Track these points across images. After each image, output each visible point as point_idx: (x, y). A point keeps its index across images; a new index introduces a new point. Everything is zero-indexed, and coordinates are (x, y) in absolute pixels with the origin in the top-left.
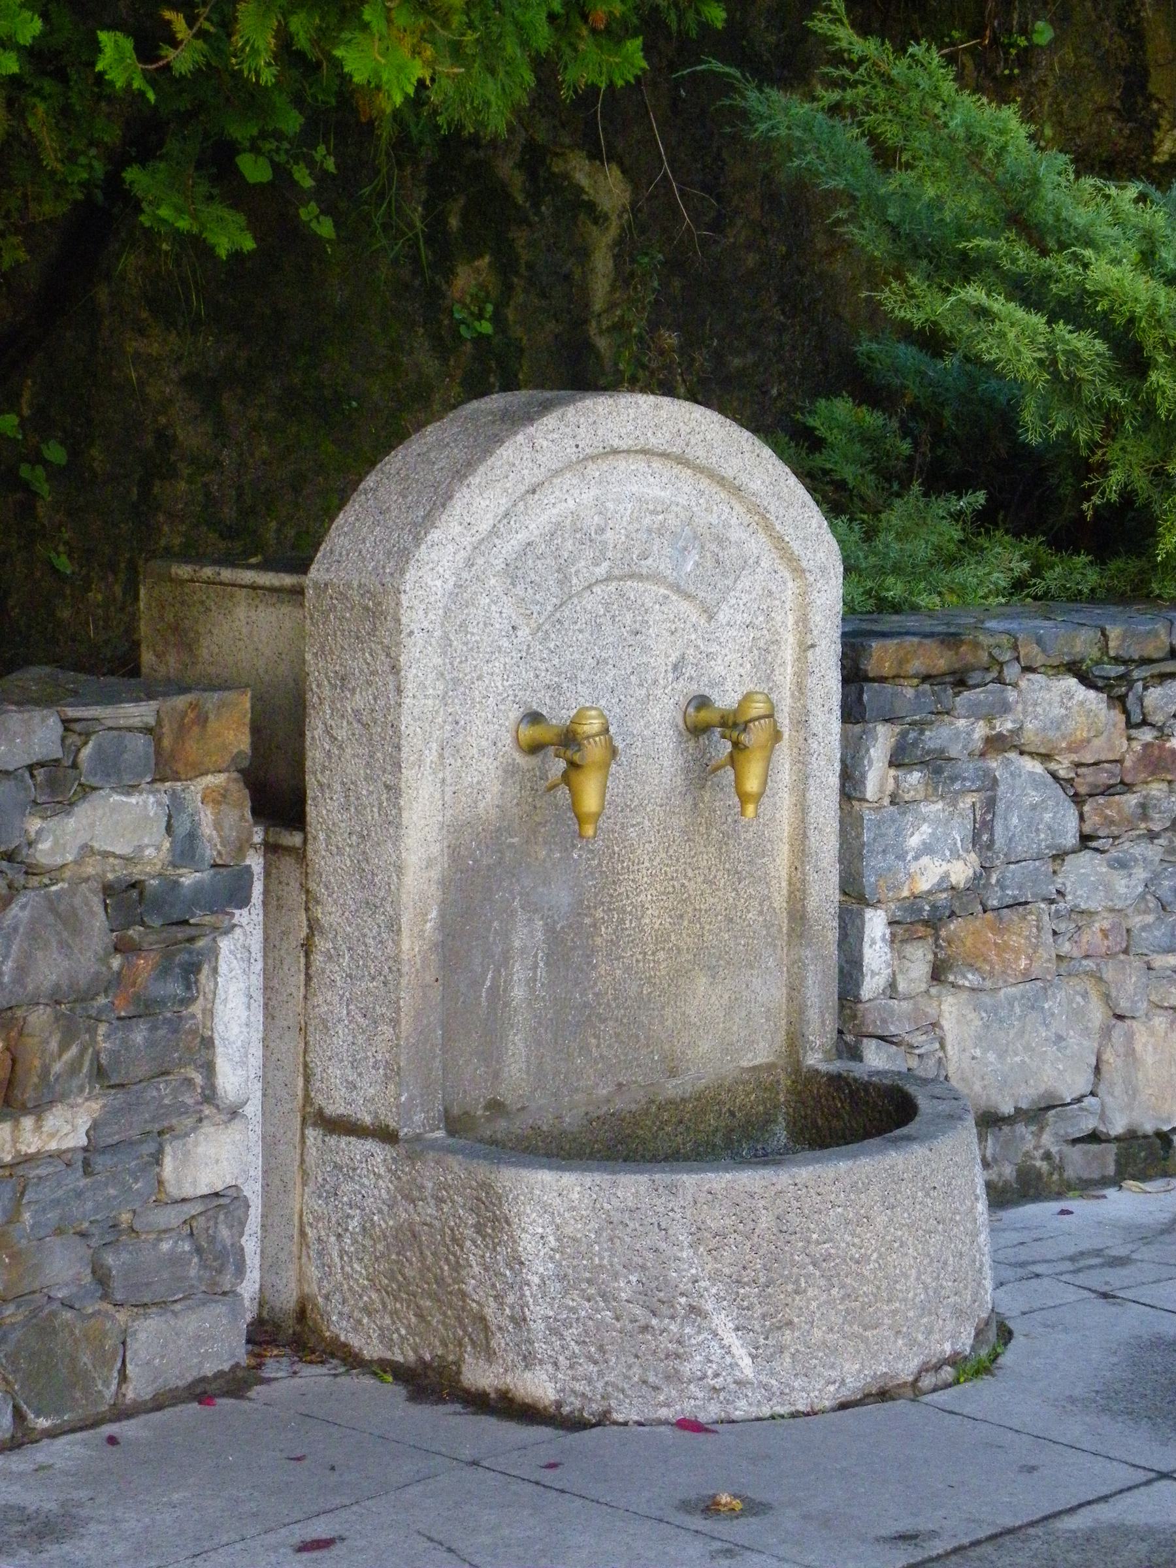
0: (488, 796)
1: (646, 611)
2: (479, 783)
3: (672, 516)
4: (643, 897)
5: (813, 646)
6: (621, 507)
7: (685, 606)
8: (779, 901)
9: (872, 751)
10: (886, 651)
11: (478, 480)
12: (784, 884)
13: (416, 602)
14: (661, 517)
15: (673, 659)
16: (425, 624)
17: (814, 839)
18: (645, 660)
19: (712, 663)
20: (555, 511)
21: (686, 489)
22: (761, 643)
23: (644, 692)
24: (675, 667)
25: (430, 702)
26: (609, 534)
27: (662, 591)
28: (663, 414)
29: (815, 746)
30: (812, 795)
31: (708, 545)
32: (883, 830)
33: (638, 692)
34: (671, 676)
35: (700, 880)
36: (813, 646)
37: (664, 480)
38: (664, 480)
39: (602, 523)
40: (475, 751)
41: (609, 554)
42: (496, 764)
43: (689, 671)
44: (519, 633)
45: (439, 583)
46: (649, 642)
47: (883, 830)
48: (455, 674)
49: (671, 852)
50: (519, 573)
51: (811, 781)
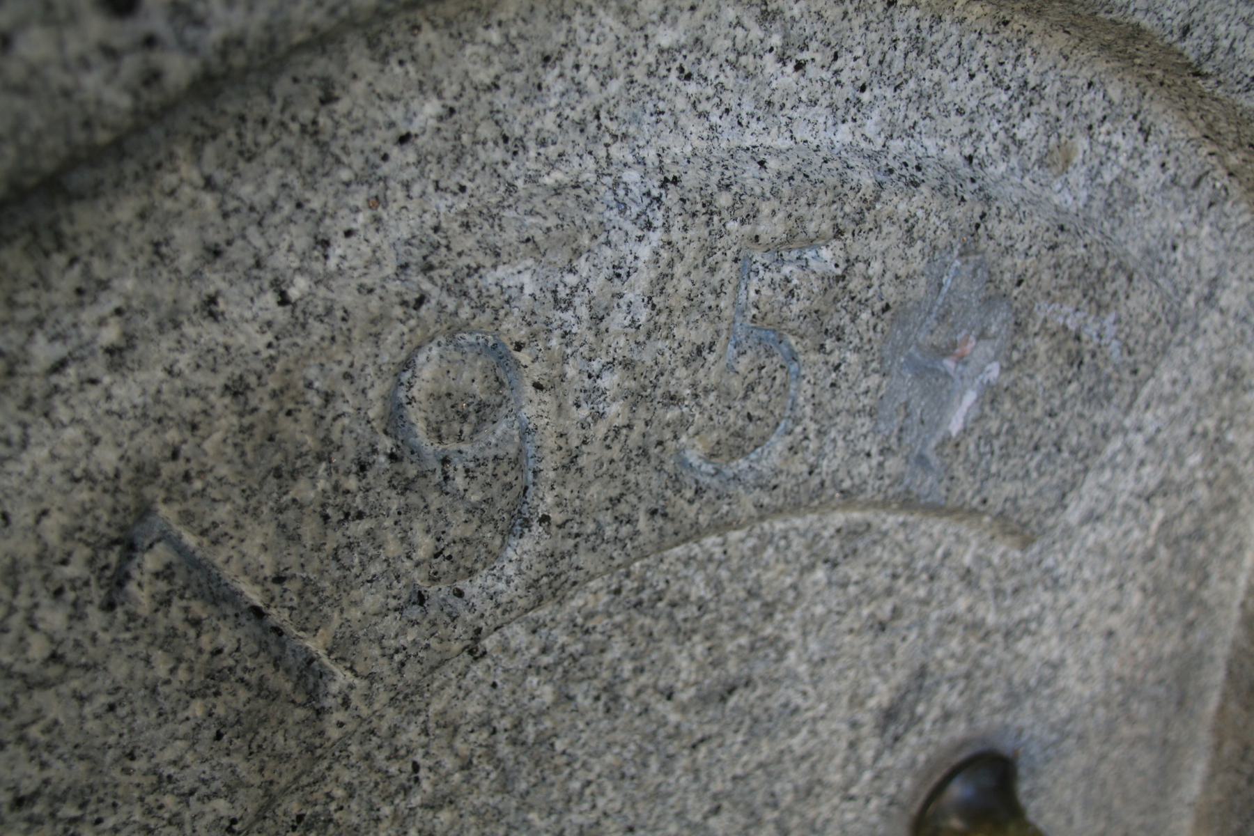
1: (768, 612)
6: (591, 274)
15: (883, 695)
20: (127, 391)
21: (959, 90)
24: (889, 715)
26: (532, 407)
31: (1043, 309)
37: (852, 68)
38: (852, 68)
39: (472, 380)
41: (545, 501)
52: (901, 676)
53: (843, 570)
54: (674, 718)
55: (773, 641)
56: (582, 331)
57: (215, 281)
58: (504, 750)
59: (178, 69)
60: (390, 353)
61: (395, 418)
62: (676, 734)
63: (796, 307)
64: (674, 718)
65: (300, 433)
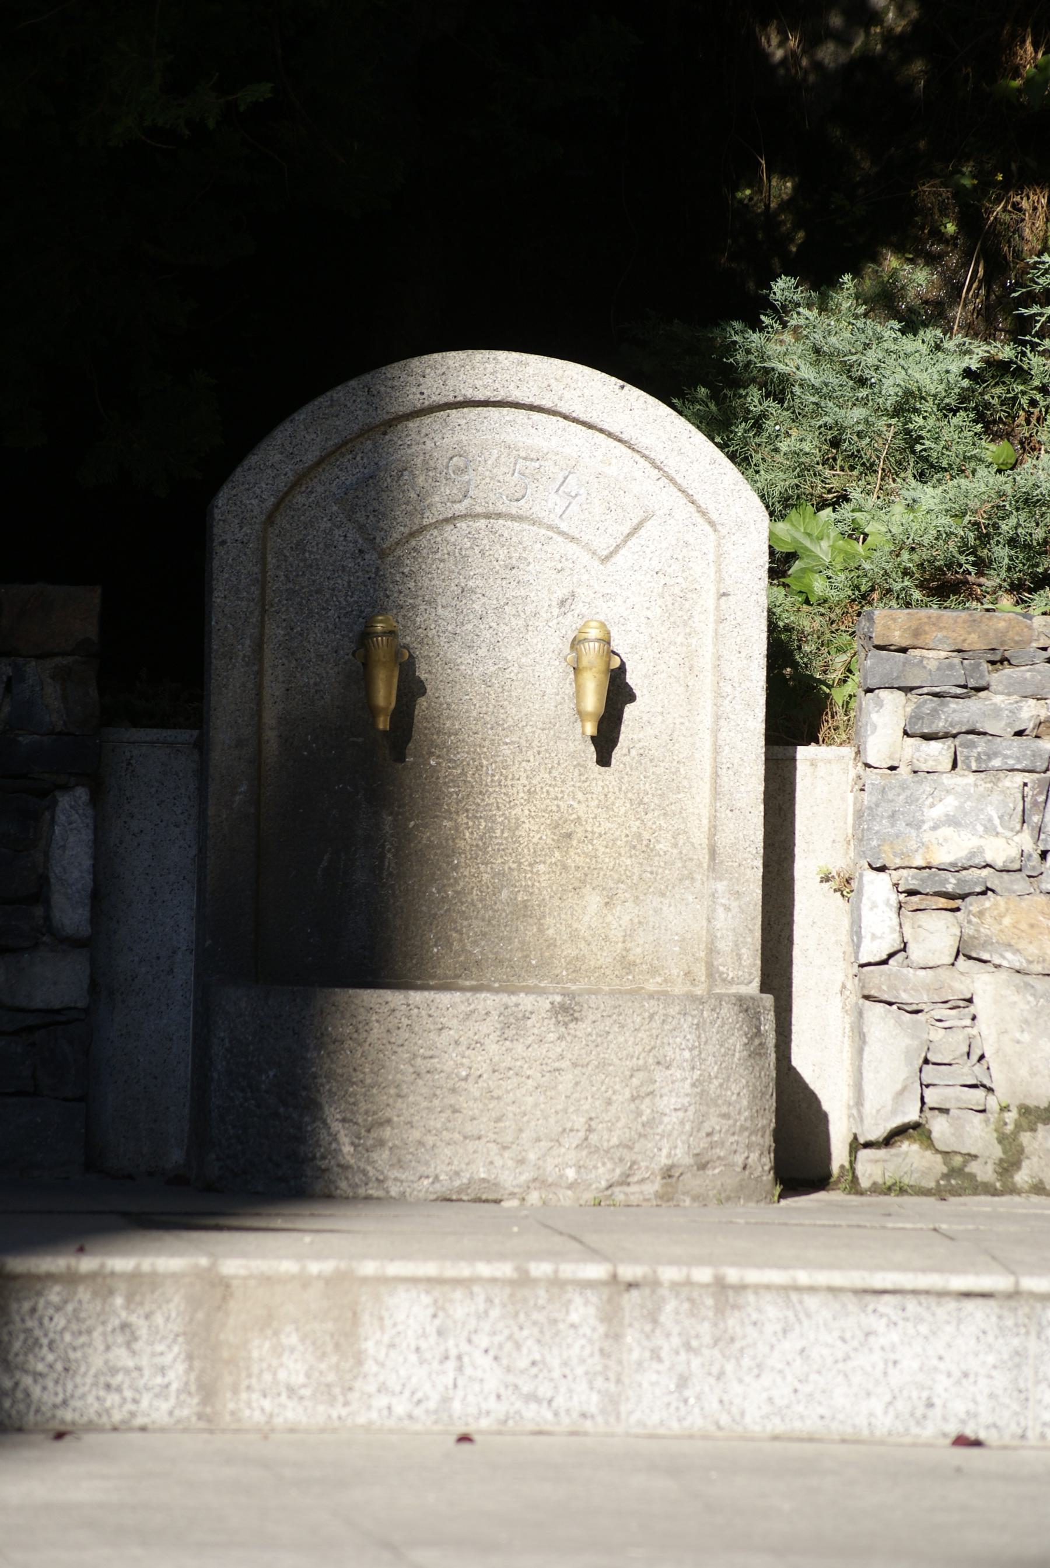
0: (327, 697)
2: (316, 684)
3: (552, 463)
4: (518, 810)
5: (724, 594)
7: (572, 549)
8: (700, 838)
9: (874, 717)
10: (894, 620)
11: (302, 417)
12: (705, 821)
13: (230, 516)
14: (537, 465)
16: (240, 536)
17: (726, 780)
18: (523, 593)
19: (611, 604)
22: (677, 590)
23: (521, 622)
24: (562, 603)
25: (244, 603)
27: (543, 531)
28: (530, 370)
29: (728, 689)
30: (722, 736)
32: (890, 796)
33: (514, 622)
34: (556, 611)
35: (593, 804)
36: (724, 594)
39: (462, 465)
40: (313, 655)
41: (471, 493)
42: (336, 669)
43: (579, 607)
44: (367, 556)
45: (254, 502)
46: (526, 578)
47: (890, 796)
48: (290, 585)
49: (555, 773)
50: (361, 502)
51: (722, 722)
52: (565, 591)
53: (545, 547)
54: (498, 568)
55: (526, 559)
56: (483, 463)
57: (425, 439)
58: (457, 555)
59: (427, 403)
60: (449, 455)
61: (447, 467)
62: (497, 573)
63: (527, 471)
64: (498, 568)
65: (431, 463)
